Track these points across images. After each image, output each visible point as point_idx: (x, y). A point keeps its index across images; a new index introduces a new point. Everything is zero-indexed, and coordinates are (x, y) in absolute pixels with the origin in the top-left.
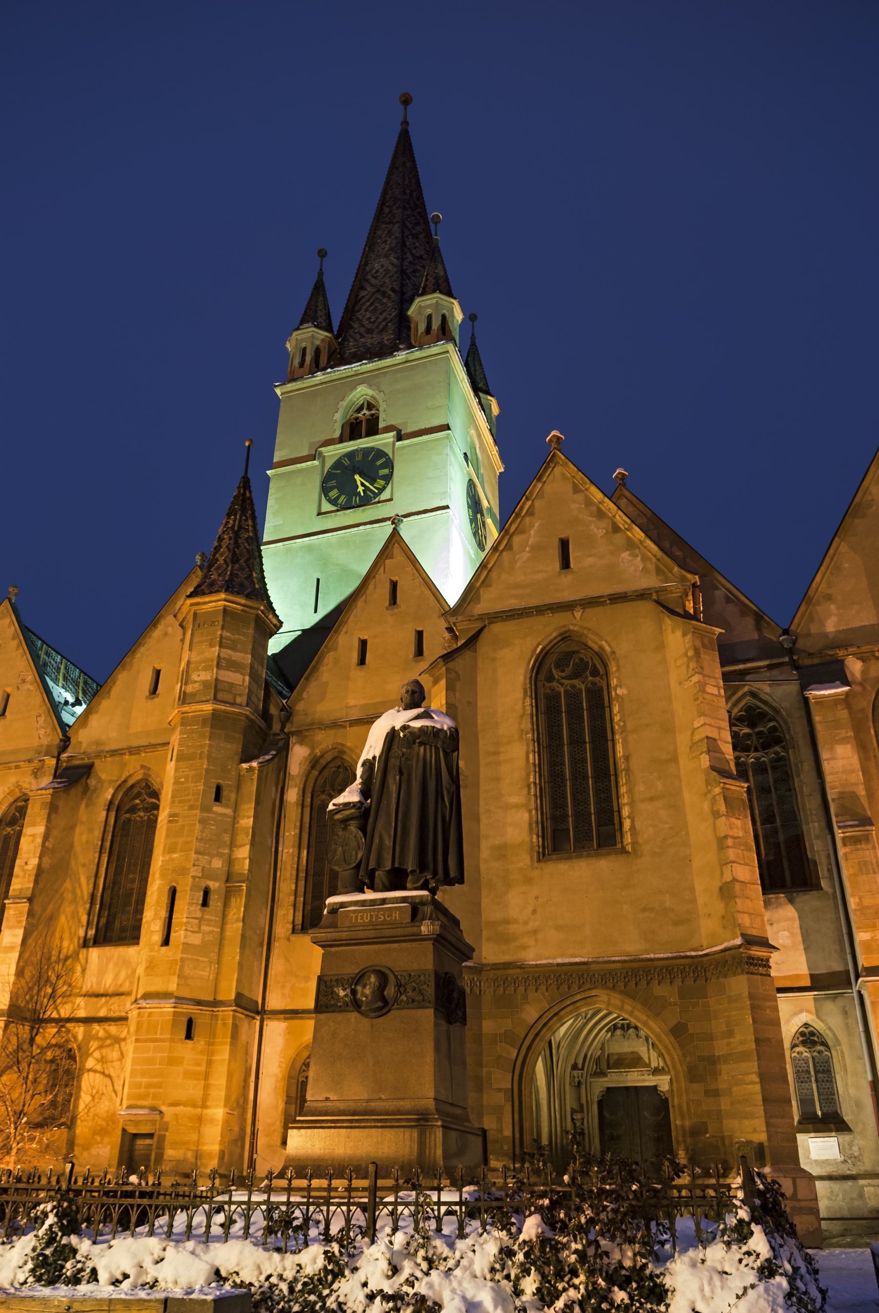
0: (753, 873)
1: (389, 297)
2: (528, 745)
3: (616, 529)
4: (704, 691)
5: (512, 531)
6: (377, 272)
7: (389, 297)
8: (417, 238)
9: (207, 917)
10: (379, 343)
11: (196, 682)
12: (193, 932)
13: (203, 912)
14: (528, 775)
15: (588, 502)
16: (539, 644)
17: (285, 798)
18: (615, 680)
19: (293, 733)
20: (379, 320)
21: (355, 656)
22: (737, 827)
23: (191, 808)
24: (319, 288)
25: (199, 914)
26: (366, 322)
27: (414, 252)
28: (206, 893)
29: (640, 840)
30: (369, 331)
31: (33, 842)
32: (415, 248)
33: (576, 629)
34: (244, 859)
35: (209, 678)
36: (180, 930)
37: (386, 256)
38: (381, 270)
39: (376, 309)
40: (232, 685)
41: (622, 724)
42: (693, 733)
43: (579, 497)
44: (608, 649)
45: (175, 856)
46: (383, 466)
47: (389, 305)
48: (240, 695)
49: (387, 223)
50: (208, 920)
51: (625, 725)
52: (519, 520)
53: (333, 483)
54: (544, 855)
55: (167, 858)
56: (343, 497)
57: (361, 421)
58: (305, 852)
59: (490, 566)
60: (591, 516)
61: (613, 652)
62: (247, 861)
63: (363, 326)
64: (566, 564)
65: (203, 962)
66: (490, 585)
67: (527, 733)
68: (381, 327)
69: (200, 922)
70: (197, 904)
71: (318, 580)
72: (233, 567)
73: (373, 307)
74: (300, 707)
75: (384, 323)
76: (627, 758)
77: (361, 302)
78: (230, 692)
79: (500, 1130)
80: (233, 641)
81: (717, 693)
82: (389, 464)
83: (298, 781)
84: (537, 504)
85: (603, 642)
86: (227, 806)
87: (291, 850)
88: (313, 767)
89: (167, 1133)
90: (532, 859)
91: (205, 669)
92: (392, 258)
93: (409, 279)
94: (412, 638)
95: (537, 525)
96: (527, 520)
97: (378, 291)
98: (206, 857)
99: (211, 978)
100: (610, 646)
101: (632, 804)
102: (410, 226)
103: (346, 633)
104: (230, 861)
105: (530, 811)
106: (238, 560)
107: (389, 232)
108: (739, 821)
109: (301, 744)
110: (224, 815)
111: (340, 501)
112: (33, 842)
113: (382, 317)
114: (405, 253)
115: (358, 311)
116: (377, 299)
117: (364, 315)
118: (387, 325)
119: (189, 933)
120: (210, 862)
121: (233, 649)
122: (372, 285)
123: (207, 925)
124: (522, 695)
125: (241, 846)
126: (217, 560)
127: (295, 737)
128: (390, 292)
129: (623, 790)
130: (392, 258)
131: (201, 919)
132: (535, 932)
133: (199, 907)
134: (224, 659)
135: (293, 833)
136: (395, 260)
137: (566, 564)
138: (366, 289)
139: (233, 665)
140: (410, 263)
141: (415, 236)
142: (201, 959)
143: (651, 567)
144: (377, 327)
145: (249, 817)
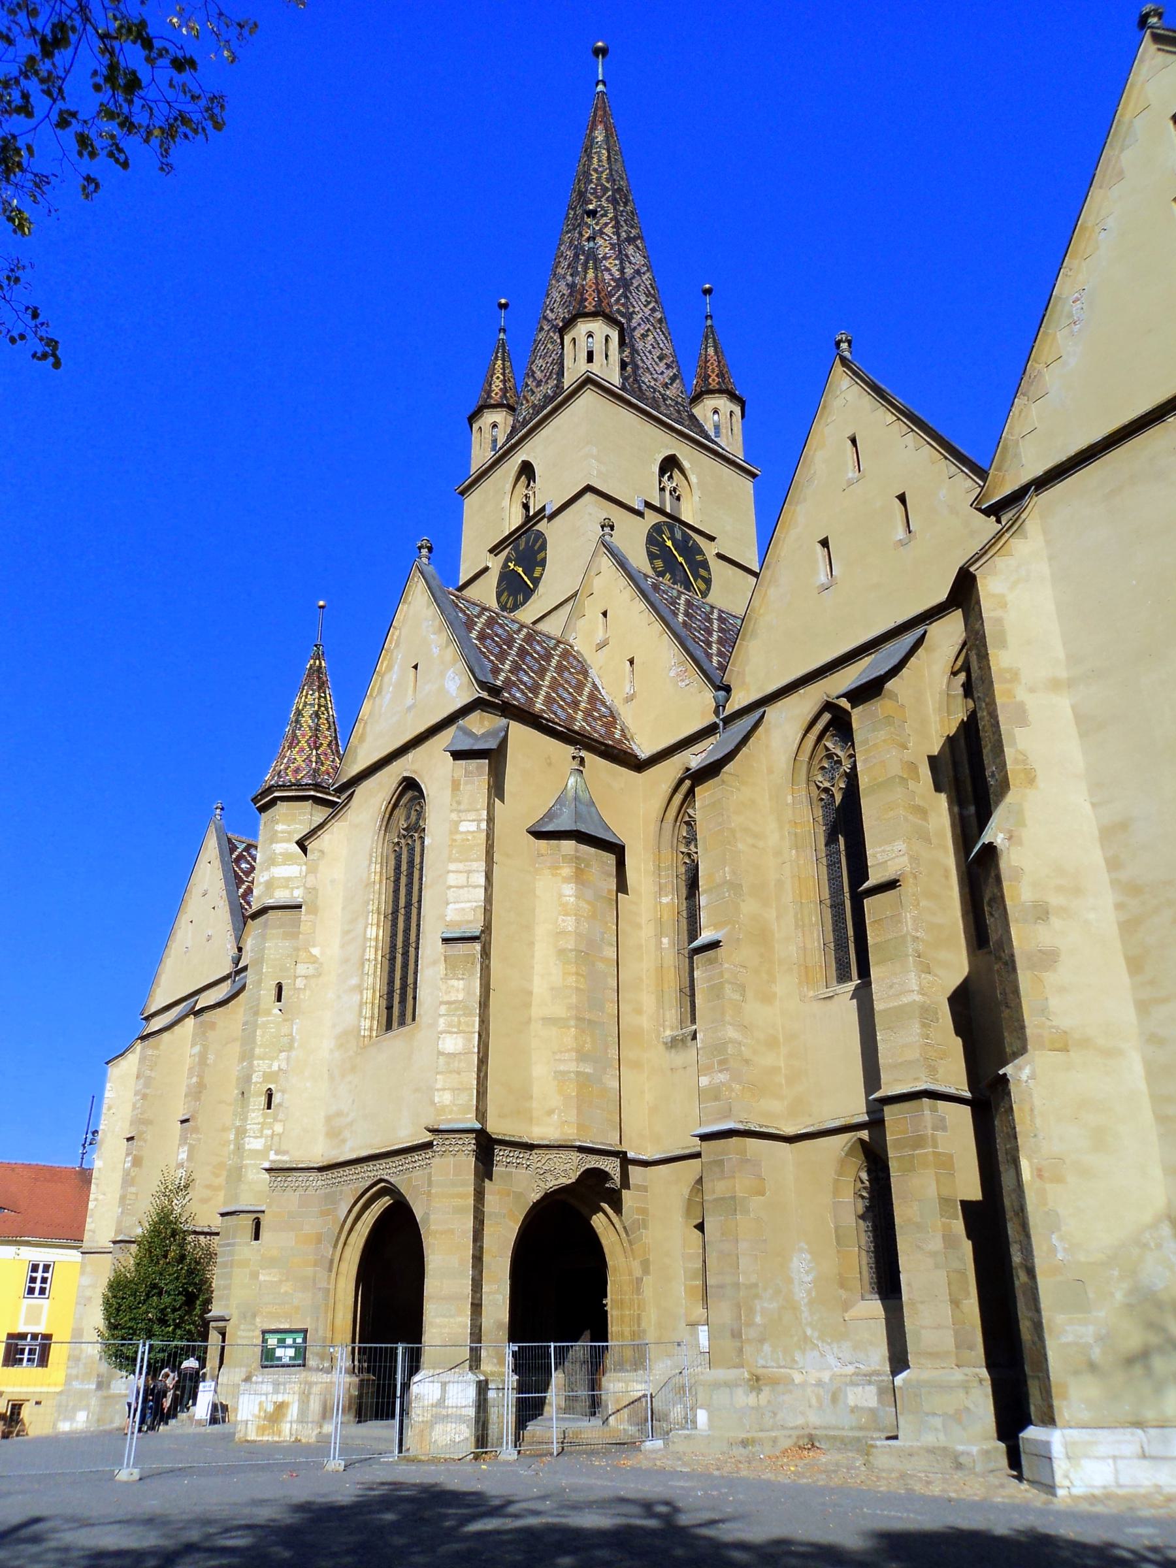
0: (470, 1040)
4: (457, 831)
8: (604, 233)
12: (256, 1137)
13: (265, 1116)
16: (384, 800)
22: (458, 990)
40: (288, 879)
48: (297, 888)
56: (511, 598)
68: (548, 374)
69: (262, 1127)
75: (551, 368)
78: (287, 887)
79: (316, 1330)
80: (289, 833)
81: (474, 829)
98: (267, 1062)
106: (299, 742)
108: (461, 982)
111: (508, 606)
134: (281, 854)
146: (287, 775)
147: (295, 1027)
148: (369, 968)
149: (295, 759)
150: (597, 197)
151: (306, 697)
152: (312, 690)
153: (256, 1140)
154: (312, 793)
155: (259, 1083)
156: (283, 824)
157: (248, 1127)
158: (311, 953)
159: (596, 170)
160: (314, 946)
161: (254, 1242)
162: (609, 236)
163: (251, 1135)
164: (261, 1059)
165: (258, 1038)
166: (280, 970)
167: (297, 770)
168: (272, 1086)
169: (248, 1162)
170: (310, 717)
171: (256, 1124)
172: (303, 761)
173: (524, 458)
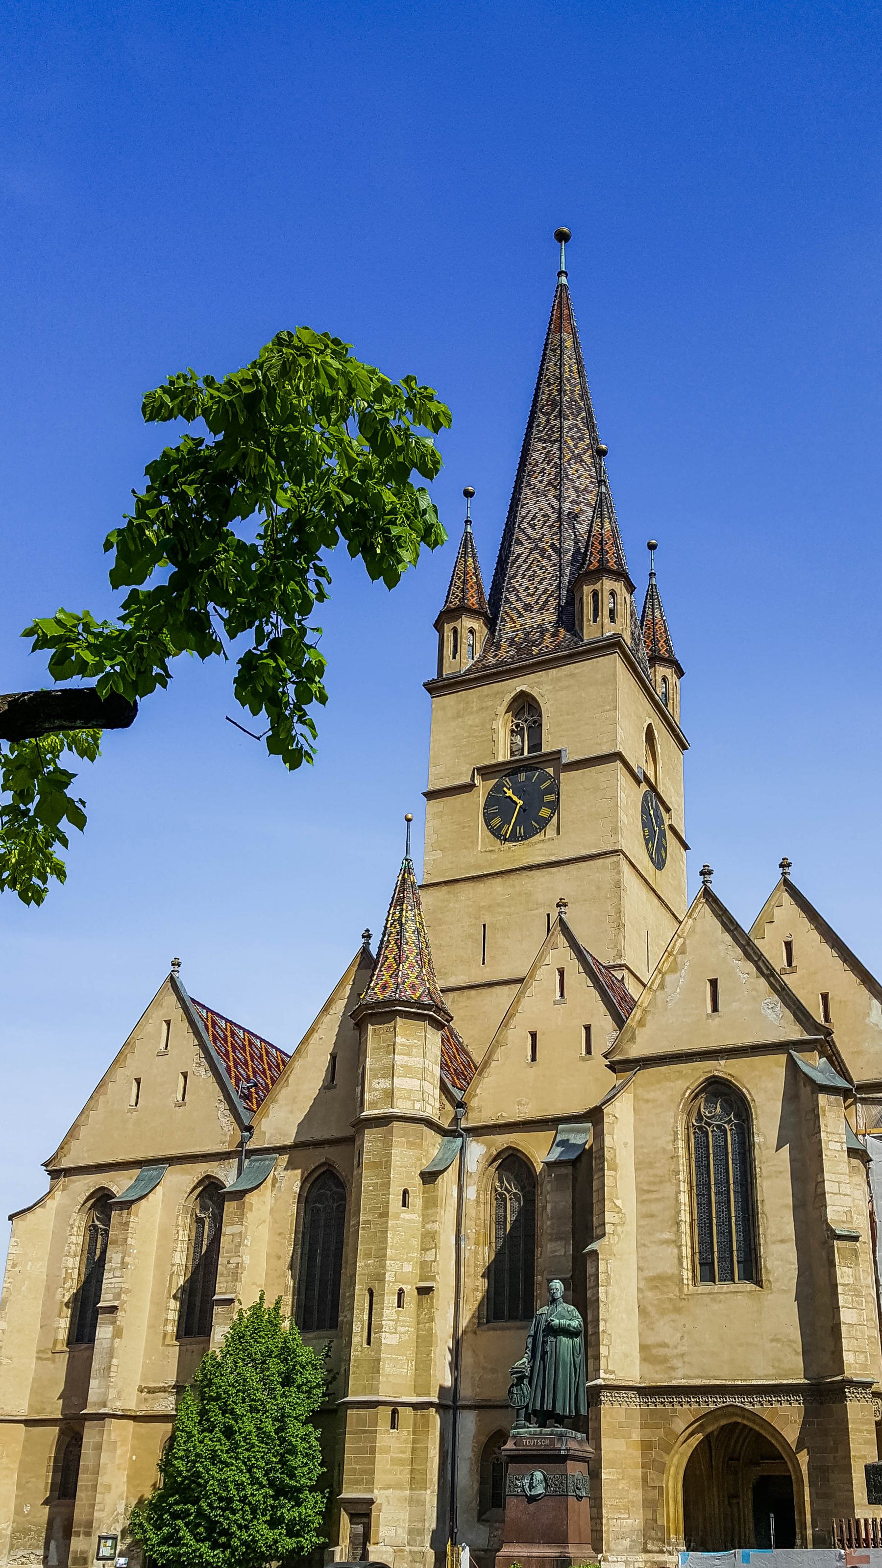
1: (549, 558)
6: (533, 519)
7: (549, 558)
8: (582, 461)
11: (376, 1090)
12: (391, 1333)
20: (539, 592)
23: (381, 1215)
26: (523, 595)
27: (577, 484)
28: (401, 1292)
30: (528, 607)
32: (578, 477)
34: (432, 1262)
40: (410, 1091)
46: (549, 791)
47: (550, 569)
50: (403, 1321)
53: (494, 809)
63: (519, 599)
65: (401, 1360)
68: (541, 602)
69: (396, 1324)
70: (392, 1307)
71: (484, 926)
73: (530, 573)
74: (474, 1103)
75: (544, 597)
78: (409, 1099)
80: (408, 1046)
83: (475, 1178)
86: (413, 1212)
91: (383, 1077)
92: (550, 497)
97: (536, 547)
98: (398, 1262)
102: (571, 444)
106: (408, 958)
110: (410, 1221)
113: (542, 588)
115: (513, 577)
117: (520, 583)
118: (547, 601)
122: (529, 538)
125: (428, 1250)
128: (550, 551)
130: (550, 497)
131: (397, 1321)
136: (555, 503)
138: (523, 545)
141: (578, 458)
149: (408, 974)
150: (572, 413)
151: (406, 912)
154: (431, 1013)
155: (393, 1282)
157: (384, 1323)
159: (568, 380)
161: (392, 1431)
162: (588, 467)
165: (389, 1240)
166: (406, 1177)
167: (413, 987)
168: (404, 1287)
172: (416, 978)
173: (524, 688)
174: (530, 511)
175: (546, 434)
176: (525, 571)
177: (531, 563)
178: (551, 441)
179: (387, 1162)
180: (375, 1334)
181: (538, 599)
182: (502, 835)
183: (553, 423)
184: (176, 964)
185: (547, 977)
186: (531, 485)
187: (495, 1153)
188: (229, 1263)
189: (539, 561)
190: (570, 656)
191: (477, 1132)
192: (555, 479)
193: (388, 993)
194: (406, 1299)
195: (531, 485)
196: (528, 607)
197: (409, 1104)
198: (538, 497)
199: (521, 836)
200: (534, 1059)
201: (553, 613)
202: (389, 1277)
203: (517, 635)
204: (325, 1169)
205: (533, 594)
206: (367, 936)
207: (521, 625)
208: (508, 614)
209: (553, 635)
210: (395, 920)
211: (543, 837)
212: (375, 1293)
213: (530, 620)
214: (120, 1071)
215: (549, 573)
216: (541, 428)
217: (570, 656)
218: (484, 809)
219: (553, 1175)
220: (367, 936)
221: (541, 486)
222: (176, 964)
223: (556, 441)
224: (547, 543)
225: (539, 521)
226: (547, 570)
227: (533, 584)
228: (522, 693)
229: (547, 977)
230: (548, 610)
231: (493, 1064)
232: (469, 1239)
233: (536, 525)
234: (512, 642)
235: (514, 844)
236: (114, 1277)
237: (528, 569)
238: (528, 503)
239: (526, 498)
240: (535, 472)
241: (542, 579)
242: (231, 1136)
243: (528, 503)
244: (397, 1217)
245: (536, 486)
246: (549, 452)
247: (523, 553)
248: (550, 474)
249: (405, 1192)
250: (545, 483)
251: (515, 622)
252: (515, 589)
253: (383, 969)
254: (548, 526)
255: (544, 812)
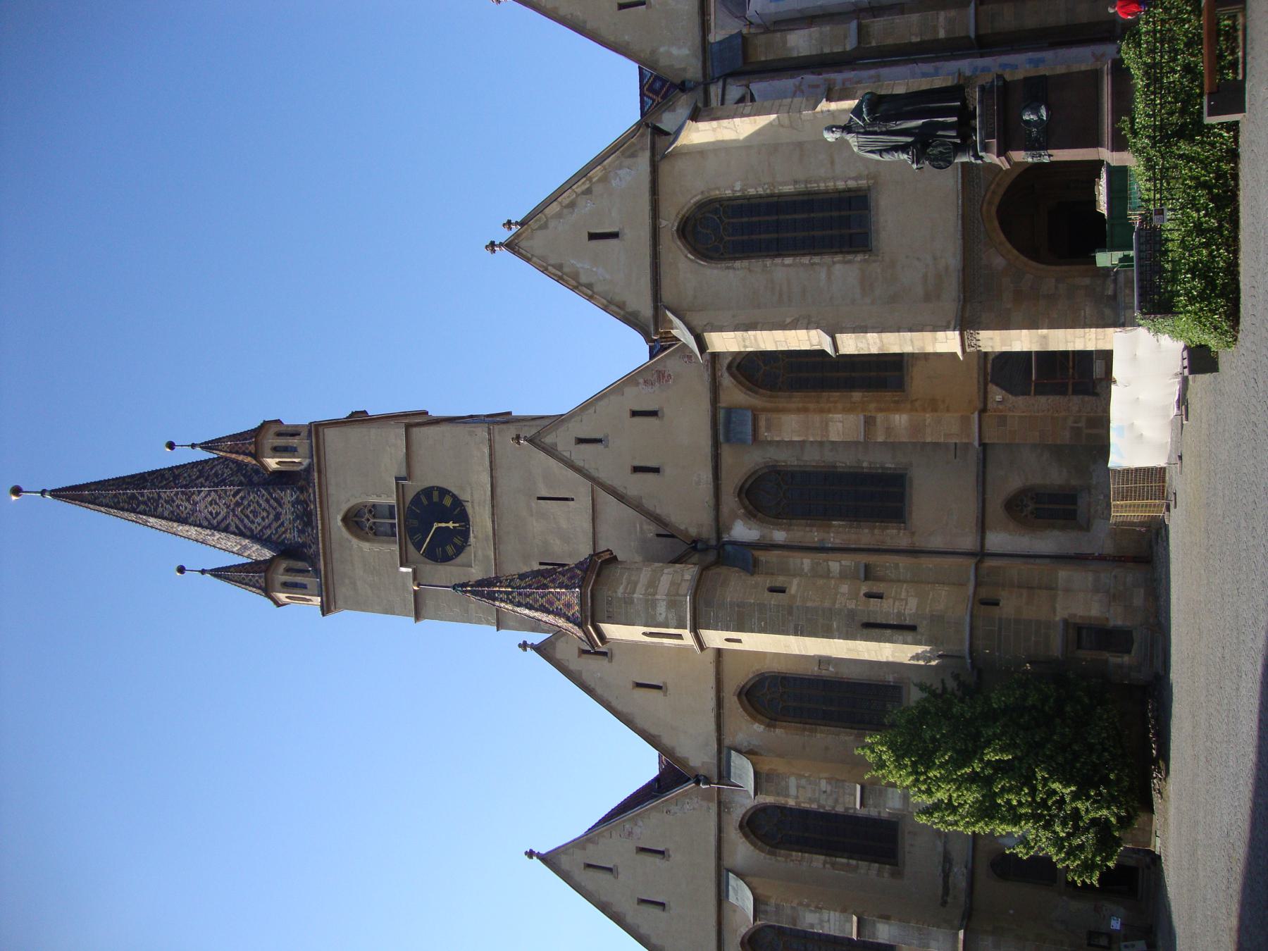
2: (776, 265)
3: (588, 192)
5: (575, 284)
6: (211, 513)
9: (893, 595)
10: (293, 506)
11: (666, 617)
12: (906, 604)
14: (803, 265)
15: (559, 216)
16: (686, 257)
17: (781, 543)
18: (727, 192)
19: (719, 537)
20: (267, 508)
21: (650, 477)
23: (790, 613)
24: (219, 573)
25: (891, 601)
27: (194, 477)
28: (869, 595)
29: (866, 173)
30: (278, 516)
31: (804, 788)
32: (190, 477)
33: (676, 224)
34: (841, 565)
35: (665, 603)
36: (904, 614)
37: (195, 504)
38: (210, 509)
39: (254, 512)
40: (672, 583)
41: (766, 186)
42: (782, 126)
43: (552, 224)
44: (697, 198)
45: (835, 626)
47: (251, 497)
48: (683, 576)
49: (158, 505)
51: (767, 184)
52: (565, 277)
53: (439, 551)
54: (871, 250)
55: (836, 633)
57: (374, 523)
58: (834, 523)
59: (605, 302)
60: (572, 213)
61: (702, 192)
62: (843, 562)
63: (269, 526)
64: (614, 235)
65: (933, 595)
66: (624, 303)
67: (765, 266)
68: (275, 505)
72: (551, 588)
74: (693, 531)
76: (796, 182)
77: (242, 528)
78: (679, 584)
80: (628, 584)
82: (428, 491)
84: (552, 262)
85: (692, 201)
87: (832, 535)
88: (755, 516)
89: (1078, 615)
90: (875, 261)
92: (197, 498)
93: (225, 479)
94: (637, 420)
95: (572, 262)
96: (566, 270)
97: (233, 510)
98: (838, 596)
99: (947, 589)
100: (695, 196)
101: (834, 179)
102: (165, 483)
103: (625, 488)
104: (843, 576)
105: (834, 263)
107: (167, 502)
108: (858, 92)
109: (731, 529)
110: (799, 585)
112: (804, 788)
113: (264, 504)
114: (196, 484)
115: (252, 531)
116: (241, 511)
118: (276, 500)
119: (908, 607)
120: (843, 594)
121: (636, 584)
123: (900, 594)
124: (731, 271)
125: (829, 570)
126: (542, 604)
127: (723, 536)
128: (238, 497)
129: (822, 186)
131: (895, 599)
132: (935, 258)
133: (884, 600)
134: (646, 590)
135: (816, 534)
137: (614, 235)
138: (229, 524)
139: (653, 584)
140: (206, 480)
142: (930, 597)
143: (628, 162)
144: (275, 509)
145: (802, 564)
146: (574, 583)
147: (848, 326)
148: (816, 259)
150: (143, 483)
151: (502, 587)
152: (497, 582)
153: (909, 604)
156: (618, 588)
158: (788, 324)
160: (785, 321)
161: (1001, 604)
163: (903, 607)
164: (834, 603)
169: (927, 610)
170: (521, 580)
171: (894, 604)
173: (339, 518)
174: (205, 517)
175: (152, 504)
176: (249, 521)
177: (244, 515)
178: (159, 499)
179: (738, 606)
180: (905, 620)
181: (273, 508)
182: (463, 545)
183: (146, 498)
184: (530, 854)
185: (583, 455)
186: (187, 517)
187: (742, 511)
188: (825, 792)
189: (244, 508)
190: (319, 472)
191: (720, 526)
192: (186, 494)
193: (575, 601)
194: (875, 590)
195: (187, 517)
196: (278, 516)
197: (683, 584)
198: (196, 511)
199: (464, 526)
200: (656, 470)
201: (285, 493)
202: (851, 605)
203: (297, 527)
204: (744, 698)
205: (268, 512)
206: (524, 646)
207: (290, 523)
208: (280, 536)
209: (302, 492)
210: (508, 598)
211: (469, 503)
212: (865, 620)
213: (287, 514)
214: (629, 919)
215: (254, 498)
216: (147, 509)
217: (319, 472)
218: (437, 561)
219: (766, 434)
220: (524, 646)
221: (189, 506)
222: (530, 854)
223: (158, 494)
224: (231, 500)
225: (214, 508)
226: (251, 500)
227: (260, 513)
228: (345, 520)
229: (583, 455)
230: (282, 498)
231: (658, 511)
232: (823, 540)
233: (216, 513)
234: (301, 532)
235: (471, 532)
236: (829, 921)
237: (247, 517)
238: (200, 520)
239: (196, 521)
240: (178, 514)
241: (258, 505)
242: (702, 800)
243: (200, 520)
244: (794, 597)
245: (188, 513)
246: (166, 501)
247: (236, 523)
248: (182, 500)
249: (773, 590)
250: (187, 504)
251: (286, 530)
252: (261, 530)
253: (551, 609)
254: (219, 499)
255: (448, 502)
